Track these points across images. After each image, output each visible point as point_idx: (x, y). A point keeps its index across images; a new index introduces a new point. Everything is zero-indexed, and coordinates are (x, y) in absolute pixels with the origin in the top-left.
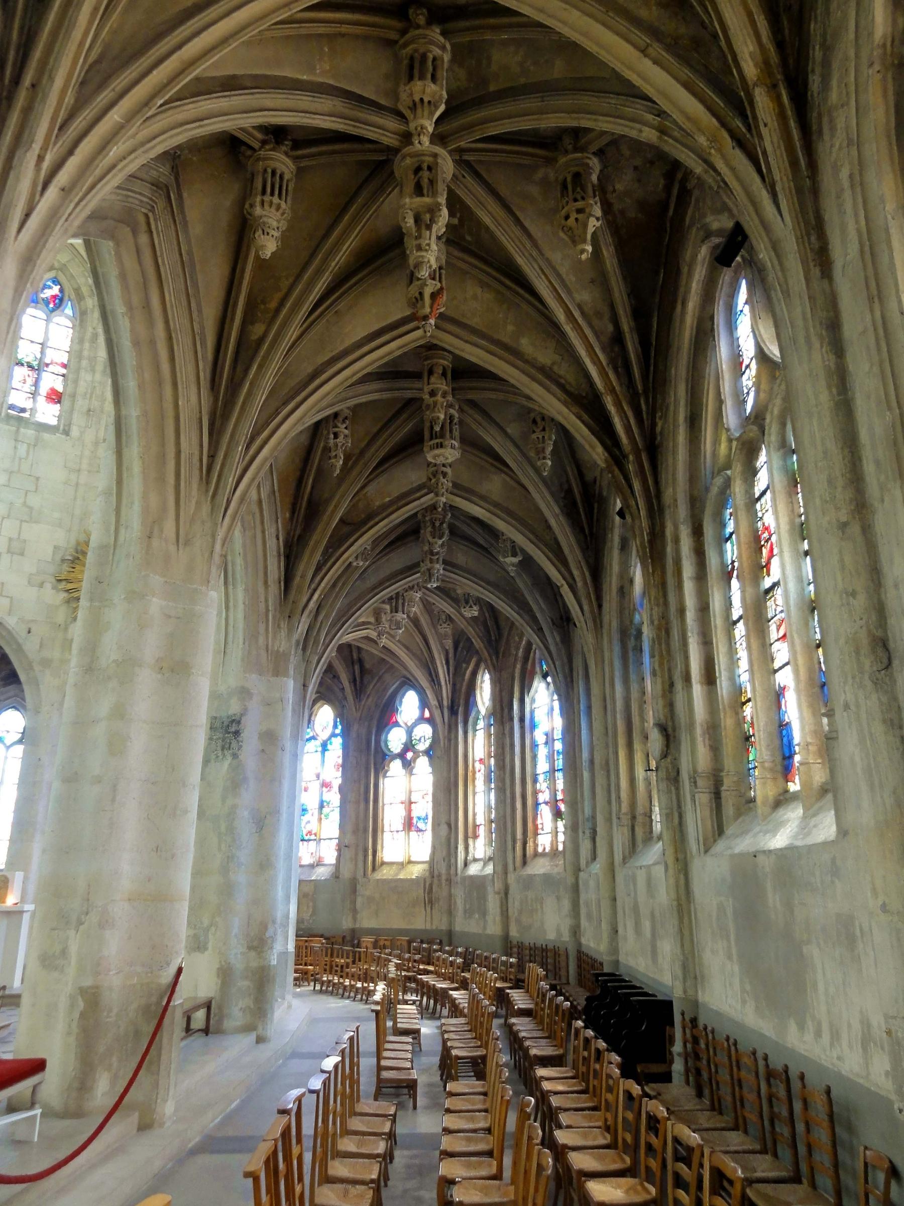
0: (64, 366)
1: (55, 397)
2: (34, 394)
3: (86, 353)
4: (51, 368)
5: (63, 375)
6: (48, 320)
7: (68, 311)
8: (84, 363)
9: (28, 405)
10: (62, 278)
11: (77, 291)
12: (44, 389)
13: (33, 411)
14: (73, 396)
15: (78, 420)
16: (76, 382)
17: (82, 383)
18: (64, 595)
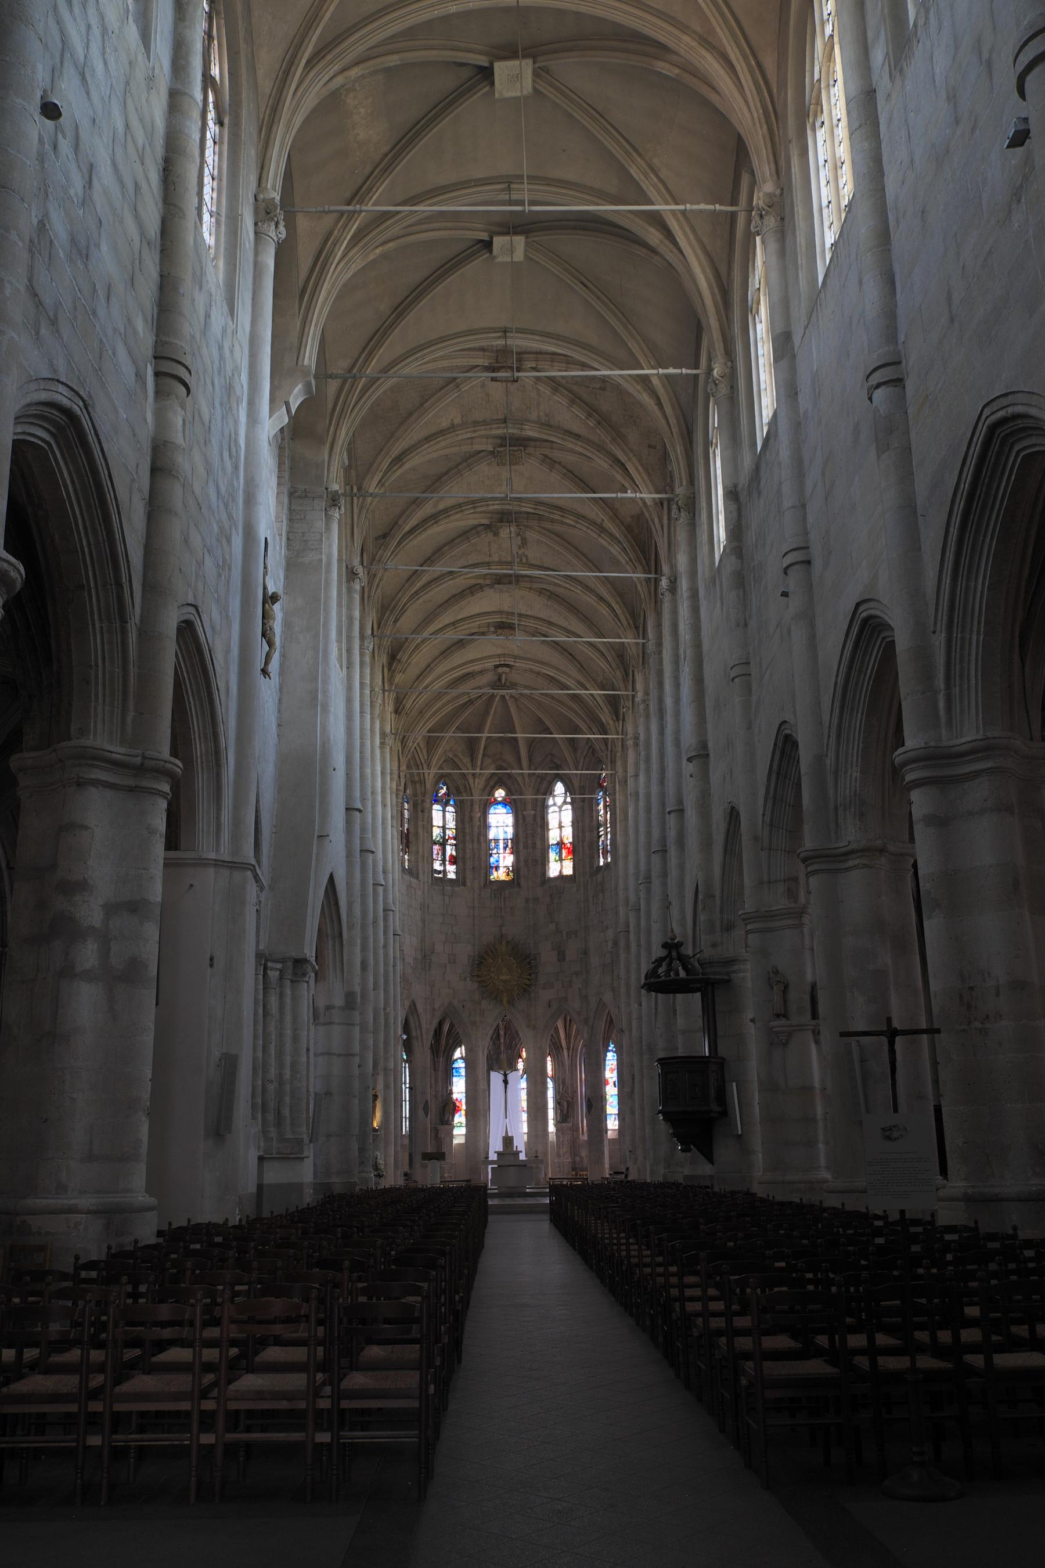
0: (455, 838)
1: (454, 860)
2: (444, 861)
3: (467, 831)
4: (450, 842)
5: (455, 845)
6: (444, 811)
7: (452, 802)
8: (468, 838)
9: (441, 868)
10: (448, 781)
11: (457, 789)
12: (447, 858)
13: (445, 872)
14: (464, 859)
15: (469, 875)
16: (464, 850)
17: (468, 851)
18: (476, 985)
